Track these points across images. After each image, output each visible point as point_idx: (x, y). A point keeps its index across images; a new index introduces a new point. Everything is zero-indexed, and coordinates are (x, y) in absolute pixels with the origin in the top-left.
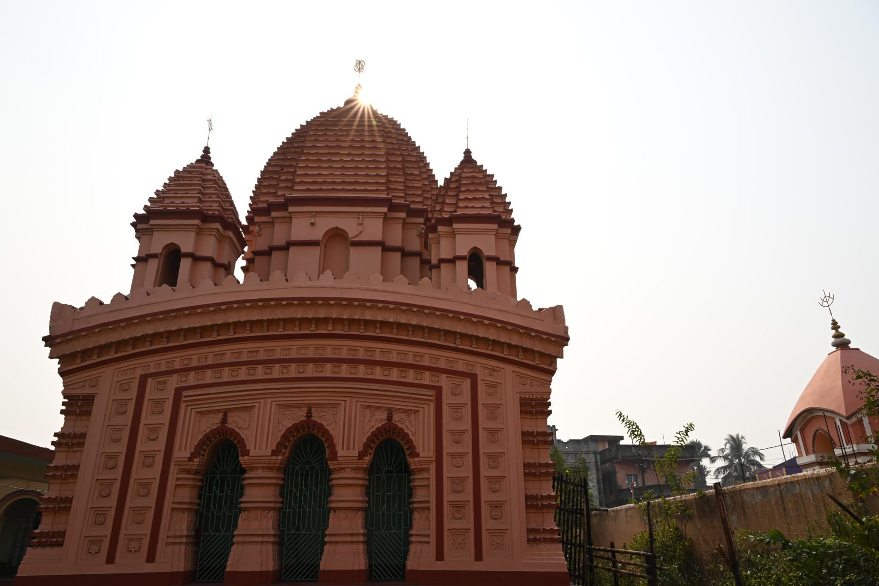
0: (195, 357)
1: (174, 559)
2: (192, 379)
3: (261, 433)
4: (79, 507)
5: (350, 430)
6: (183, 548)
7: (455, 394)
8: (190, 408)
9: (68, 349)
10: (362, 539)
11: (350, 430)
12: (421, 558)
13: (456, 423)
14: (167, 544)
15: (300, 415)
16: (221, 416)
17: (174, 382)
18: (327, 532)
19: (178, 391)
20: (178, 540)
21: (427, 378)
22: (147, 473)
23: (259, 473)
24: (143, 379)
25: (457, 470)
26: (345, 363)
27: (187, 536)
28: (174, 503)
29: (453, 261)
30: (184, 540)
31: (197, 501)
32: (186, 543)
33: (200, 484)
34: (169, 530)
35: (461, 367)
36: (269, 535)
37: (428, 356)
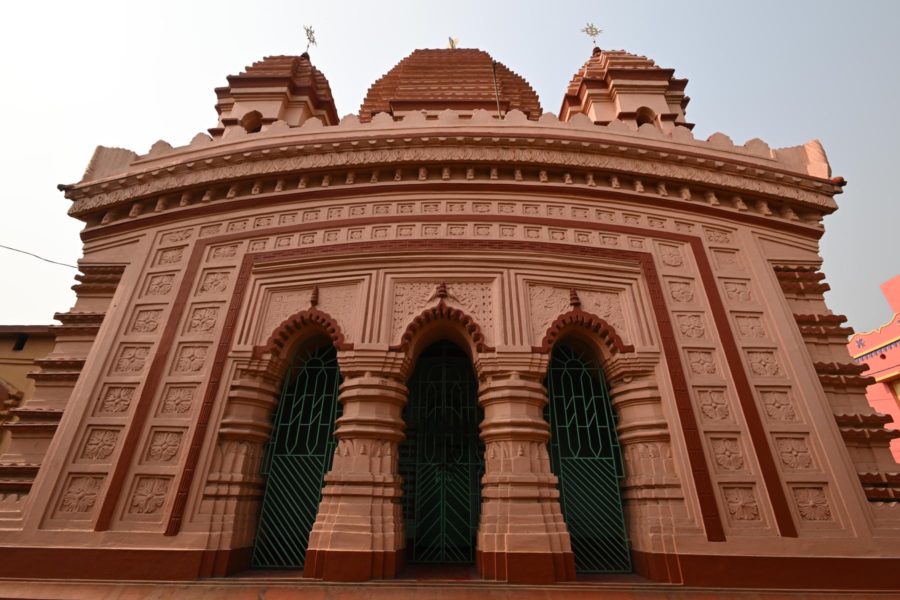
4: (65, 428)
6: (233, 503)
8: (258, 282)
9: (91, 204)
10: (556, 493)
14: (206, 497)
16: (308, 295)
18: (484, 480)
20: (224, 490)
23: (366, 379)
26: (496, 221)
27: (241, 484)
28: (223, 425)
30: (236, 490)
31: (266, 424)
32: (239, 498)
33: (271, 399)
34: (211, 471)
35: (669, 227)
36: (385, 485)
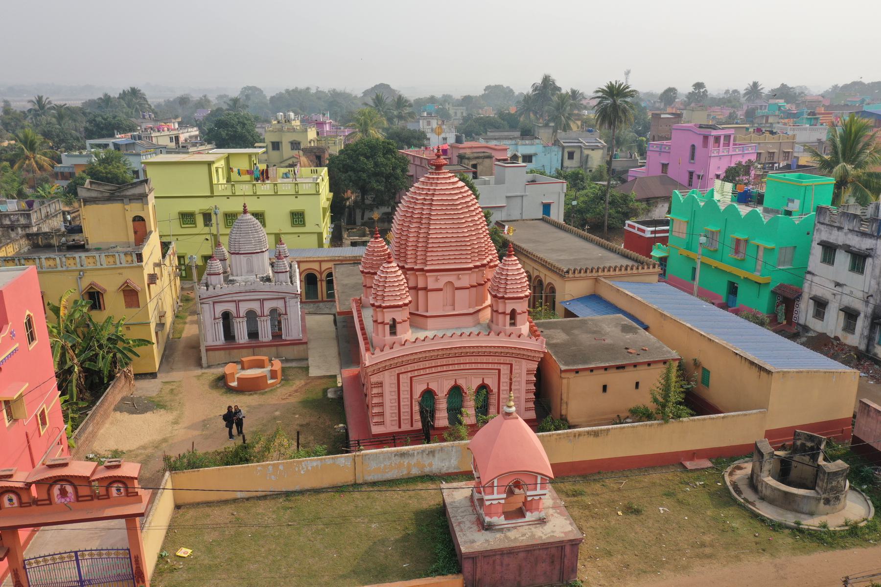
0: (416, 366)
1: (418, 425)
2: (416, 373)
3: (442, 388)
5: (470, 384)
7: (505, 370)
11: (470, 384)
13: (505, 379)
15: (453, 383)
17: (410, 375)
19: (411, 378)
21: (496, 366)
22: (405, 402)
24: (398, 375)
29: (504, 313)
37: (496, 359)
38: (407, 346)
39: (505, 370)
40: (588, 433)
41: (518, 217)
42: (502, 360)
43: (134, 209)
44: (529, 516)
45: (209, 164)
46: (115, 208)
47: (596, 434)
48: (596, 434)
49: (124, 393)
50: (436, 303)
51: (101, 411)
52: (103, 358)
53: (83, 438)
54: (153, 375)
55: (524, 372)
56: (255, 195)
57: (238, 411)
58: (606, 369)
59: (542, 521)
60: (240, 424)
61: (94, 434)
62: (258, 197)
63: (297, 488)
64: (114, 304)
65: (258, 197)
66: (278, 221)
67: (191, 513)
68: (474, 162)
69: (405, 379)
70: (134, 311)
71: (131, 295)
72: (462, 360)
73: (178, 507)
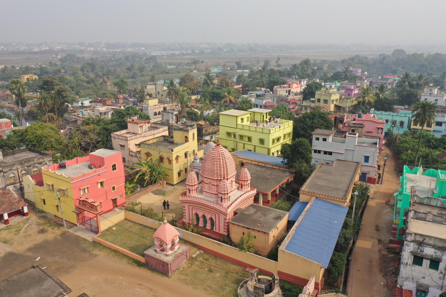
0: (193, 205)
3: (200, 215)
7: (217, 215)
12: (214, 230)
13: (217, 218)
22: (191, 215)
25: (217, 224)
38: (190, 198)
39: (217, 215)
40: (217, 243)
41: (351, 160)
42: (216, 212)
43: (185, 134)
44: (164, 252)
45: (237, 117)
46: (181, 132)
47: (219, 244)
48: (219, 244)
49: (159, 188)
50: (206, 187)
51: (144, 191)
52: (155, 177)
53: (133, 197)
54: (173, 185)
55: (223, 219)
56: (249, 130)
57: (168, 202)
58: (243, 227)
59: (167, 255)
60: (168, 205)
61: (139, 197)
62: (250, 131)
63: (148, 225)
64: (166, 161)
65: (250, 131)
66: (256, 141)
67: (126, 222)
68: (353, 129)
69: (191, 207)
70: (170, 165)
71: (170, 162)
72: (205, 207)
73: (126, 219)
